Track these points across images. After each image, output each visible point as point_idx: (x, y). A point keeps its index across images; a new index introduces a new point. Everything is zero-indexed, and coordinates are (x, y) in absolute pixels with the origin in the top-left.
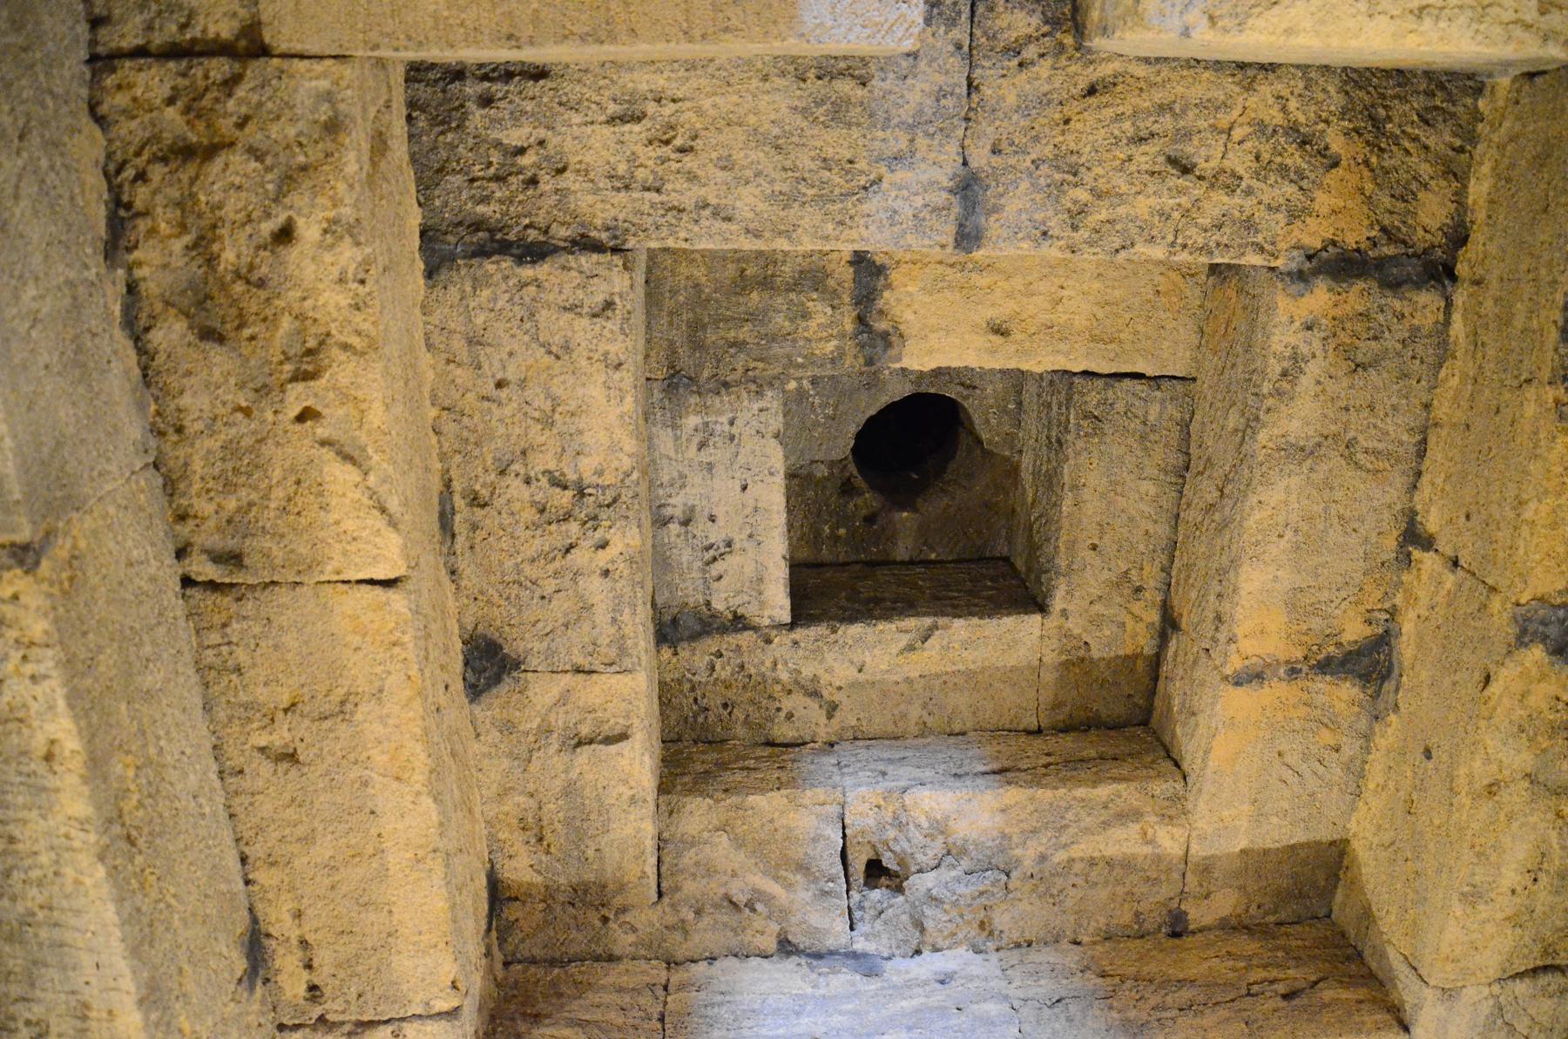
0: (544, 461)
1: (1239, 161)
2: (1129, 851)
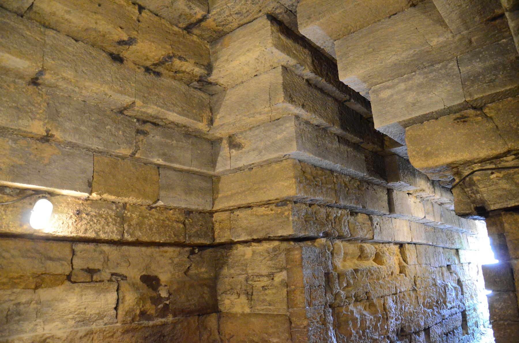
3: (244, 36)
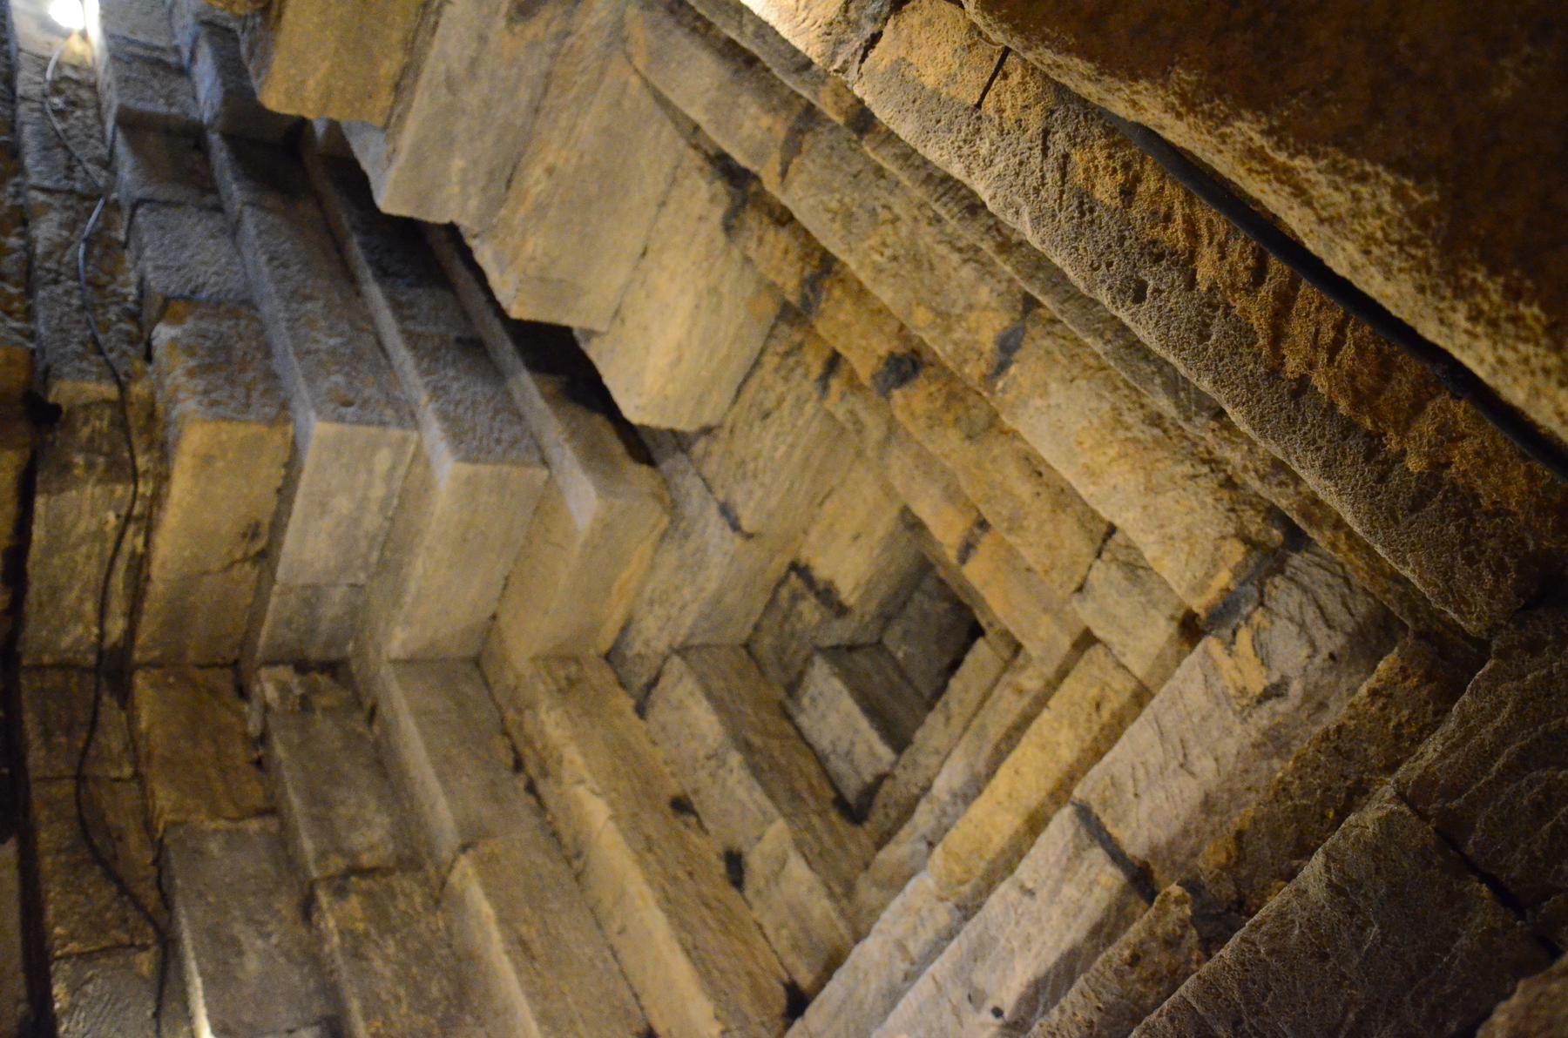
0: (702, 754)
1: (780, 388)
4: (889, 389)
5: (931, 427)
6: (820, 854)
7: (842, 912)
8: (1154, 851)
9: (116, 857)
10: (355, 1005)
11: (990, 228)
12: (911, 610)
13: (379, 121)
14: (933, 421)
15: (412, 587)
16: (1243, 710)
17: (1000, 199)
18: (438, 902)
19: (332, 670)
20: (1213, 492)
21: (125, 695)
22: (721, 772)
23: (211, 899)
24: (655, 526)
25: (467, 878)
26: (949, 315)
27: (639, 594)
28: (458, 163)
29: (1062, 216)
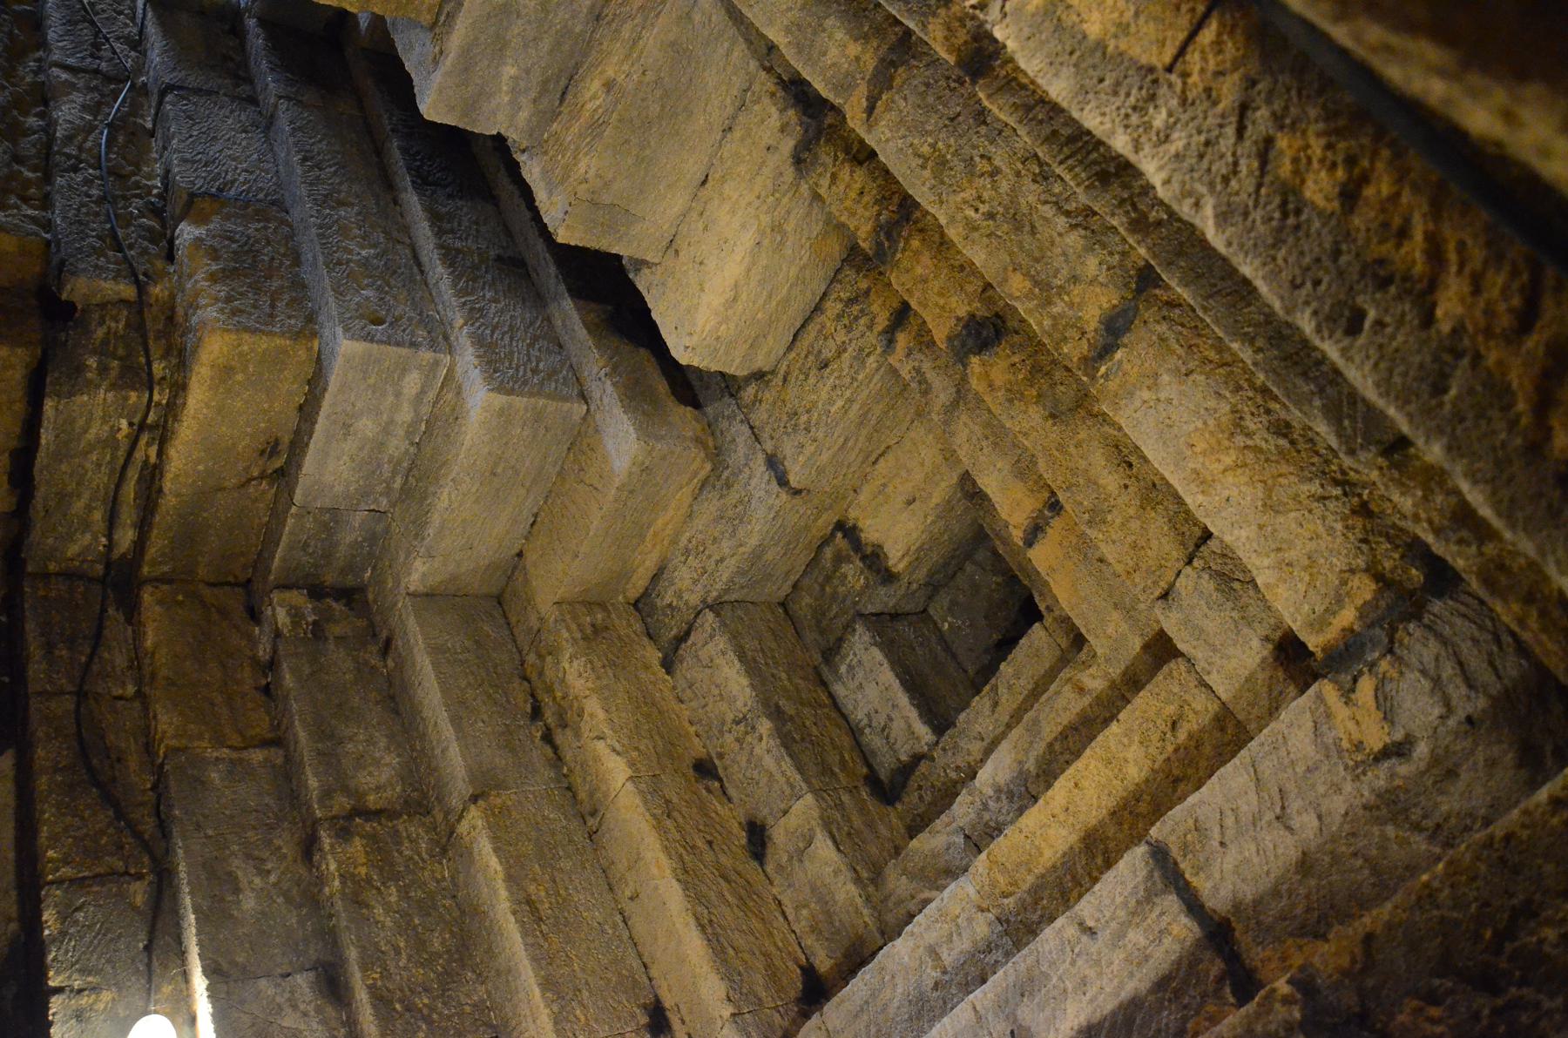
0: (730, 717)
1: (841, 337)
2: (1078, 710)
3: (786, 301)
4: (966, 355)
5: (1011, 401)
6: (849, 834)
7: (868, 899)
8: (1237, 906)
9: (114, 779)
10: (353, 954)
11: (1122, 202)
12: (961, 580)
13: (426, 18)
14: (1014, 395)
15: (436, 519)
16: (1357, 765)
17: (1176, 185)
18: (444, 851)
19: (348, 598)
20: (1344, 519)
21: (131, 610)
22: (749, 738)
23: (210, 832)
24: (695, 474)
25: (474, 826)
26: (1049, 286)
27: (674, 542)
28: (510, 71)
29: (1257, 215)
